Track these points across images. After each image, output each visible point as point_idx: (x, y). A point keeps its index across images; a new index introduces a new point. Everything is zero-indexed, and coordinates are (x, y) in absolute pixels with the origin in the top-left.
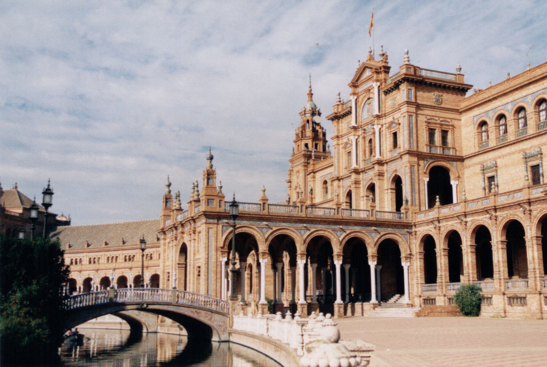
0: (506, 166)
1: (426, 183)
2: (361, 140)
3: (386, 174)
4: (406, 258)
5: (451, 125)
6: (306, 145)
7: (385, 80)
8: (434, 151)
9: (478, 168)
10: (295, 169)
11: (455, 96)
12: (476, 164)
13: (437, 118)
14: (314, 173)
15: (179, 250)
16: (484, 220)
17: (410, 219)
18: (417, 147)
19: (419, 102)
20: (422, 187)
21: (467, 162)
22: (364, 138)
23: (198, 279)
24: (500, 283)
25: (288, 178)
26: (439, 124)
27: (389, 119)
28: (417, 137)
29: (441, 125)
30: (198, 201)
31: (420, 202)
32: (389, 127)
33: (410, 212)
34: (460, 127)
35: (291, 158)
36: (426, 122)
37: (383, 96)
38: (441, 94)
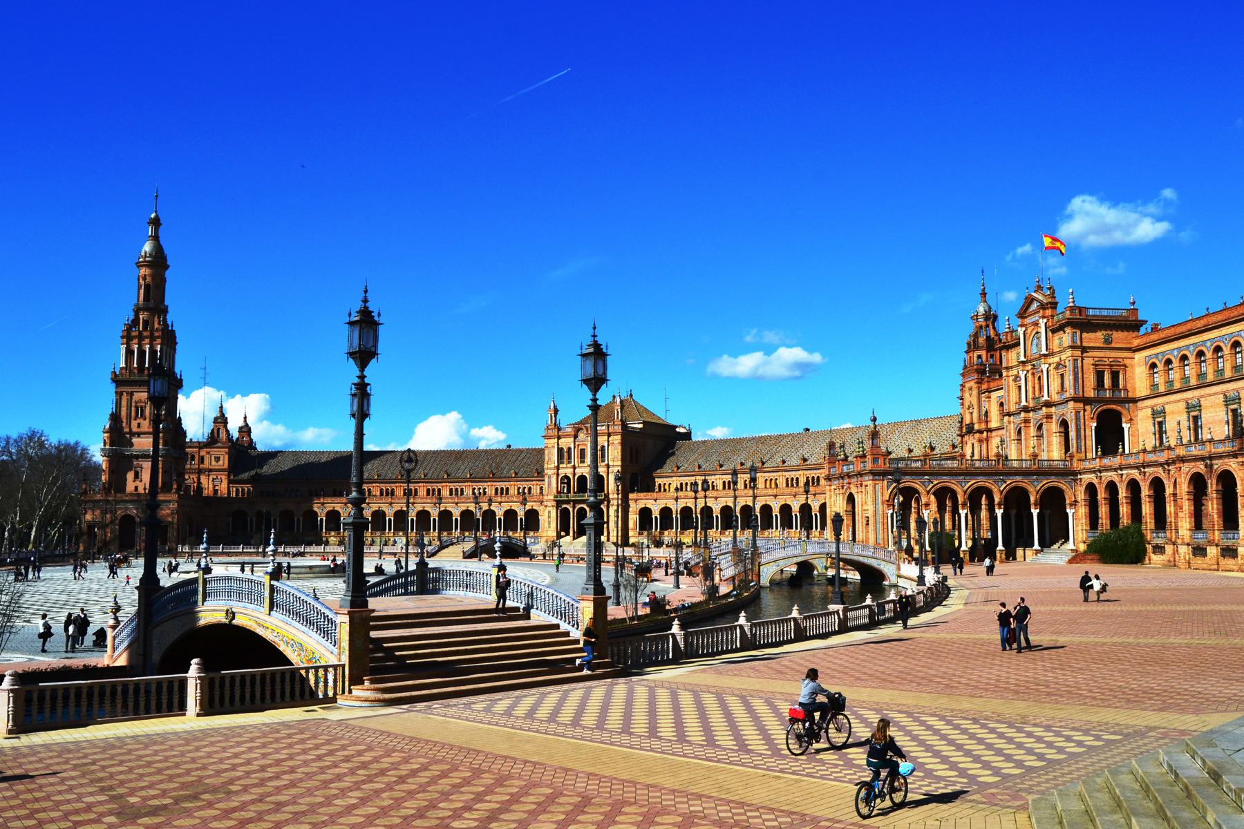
0: (1173, 413)
2: (1029, 375)
4: (1071, 505)
6: (979, 357)
7: (1052, 316)
8: (1102, 394)
9: (1149, 411)
10: (968, 385)
16: (1135, 473)
17: (1076, 465)
19: (1085, 344)
25: (959, 394)
27: (1056, 359)
32: (1057, 368)
34: (1132, 366)
37: (1050, 334)
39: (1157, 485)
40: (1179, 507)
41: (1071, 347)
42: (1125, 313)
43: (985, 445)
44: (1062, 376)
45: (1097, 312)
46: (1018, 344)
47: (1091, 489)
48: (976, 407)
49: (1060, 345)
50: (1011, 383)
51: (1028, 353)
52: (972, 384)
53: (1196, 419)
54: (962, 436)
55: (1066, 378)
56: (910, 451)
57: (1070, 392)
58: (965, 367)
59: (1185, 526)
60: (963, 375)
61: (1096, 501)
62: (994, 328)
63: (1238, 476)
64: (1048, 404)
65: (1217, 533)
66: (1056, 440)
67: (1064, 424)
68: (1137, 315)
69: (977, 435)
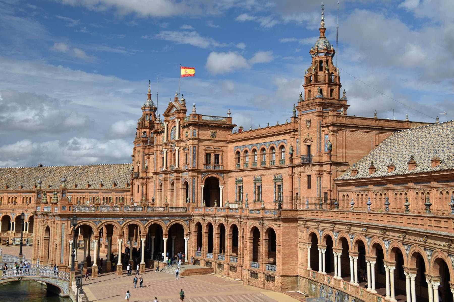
1: (202, 188)
2: (169, 152)
3: (181, 179)
4: (187, 235)
5: (221, 151)
7: (183, 118)
9: (234, 180)
10: (137, 149)
11: (224, 131)
12: (233, 177)
13: (212, 147)
14: (149, 155)
15: (45, 229)
16: (222, 220)
17: (191, 211)
18: (198, 166)
19: (200, 137)
20: (199, 191)
21: (229, 174)
22: (171, 151)
23: (56, 251)
24: (227, 258)
26: (213, 150)
27: (183, 144)
28: (198, 160)
29: (215, 151)
30: (56, 204)
31: (197, 200)
32: (184, 150)
33: (191, 207)
34: (227, 151)
35: (134, 140)
36: (204, 150)
37: (181, 128)
38: (215, 131)
39: (234, 229)
40: (245, 247)
41: (192, 139)
42: (224, 120)
43: (145, 187)
44: (186, 154)
45: (208, 118)
46: (163, 132)
47: (199, 226)
48: (141, 163)
49: (187, 136)
50: (159, 155)
51: (169, 138)
52: (140, 149)
53: (259, 187)
54: (133, 180)
55: (188, 156)
56: (102, 185)
57: (190, 167)
58: (136, 138)
59: (248, 257)
60: (135, 143)
61: (201, 234)
62: (155, 115)
63: (277, 232)
64: (178, 172)
65: (264, 264)
66: (182, 193)
67: (186, 184)
68: (231, 121)
69: (141, 180)
